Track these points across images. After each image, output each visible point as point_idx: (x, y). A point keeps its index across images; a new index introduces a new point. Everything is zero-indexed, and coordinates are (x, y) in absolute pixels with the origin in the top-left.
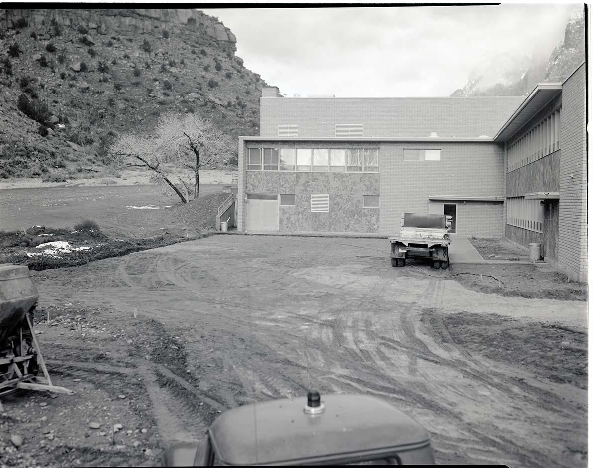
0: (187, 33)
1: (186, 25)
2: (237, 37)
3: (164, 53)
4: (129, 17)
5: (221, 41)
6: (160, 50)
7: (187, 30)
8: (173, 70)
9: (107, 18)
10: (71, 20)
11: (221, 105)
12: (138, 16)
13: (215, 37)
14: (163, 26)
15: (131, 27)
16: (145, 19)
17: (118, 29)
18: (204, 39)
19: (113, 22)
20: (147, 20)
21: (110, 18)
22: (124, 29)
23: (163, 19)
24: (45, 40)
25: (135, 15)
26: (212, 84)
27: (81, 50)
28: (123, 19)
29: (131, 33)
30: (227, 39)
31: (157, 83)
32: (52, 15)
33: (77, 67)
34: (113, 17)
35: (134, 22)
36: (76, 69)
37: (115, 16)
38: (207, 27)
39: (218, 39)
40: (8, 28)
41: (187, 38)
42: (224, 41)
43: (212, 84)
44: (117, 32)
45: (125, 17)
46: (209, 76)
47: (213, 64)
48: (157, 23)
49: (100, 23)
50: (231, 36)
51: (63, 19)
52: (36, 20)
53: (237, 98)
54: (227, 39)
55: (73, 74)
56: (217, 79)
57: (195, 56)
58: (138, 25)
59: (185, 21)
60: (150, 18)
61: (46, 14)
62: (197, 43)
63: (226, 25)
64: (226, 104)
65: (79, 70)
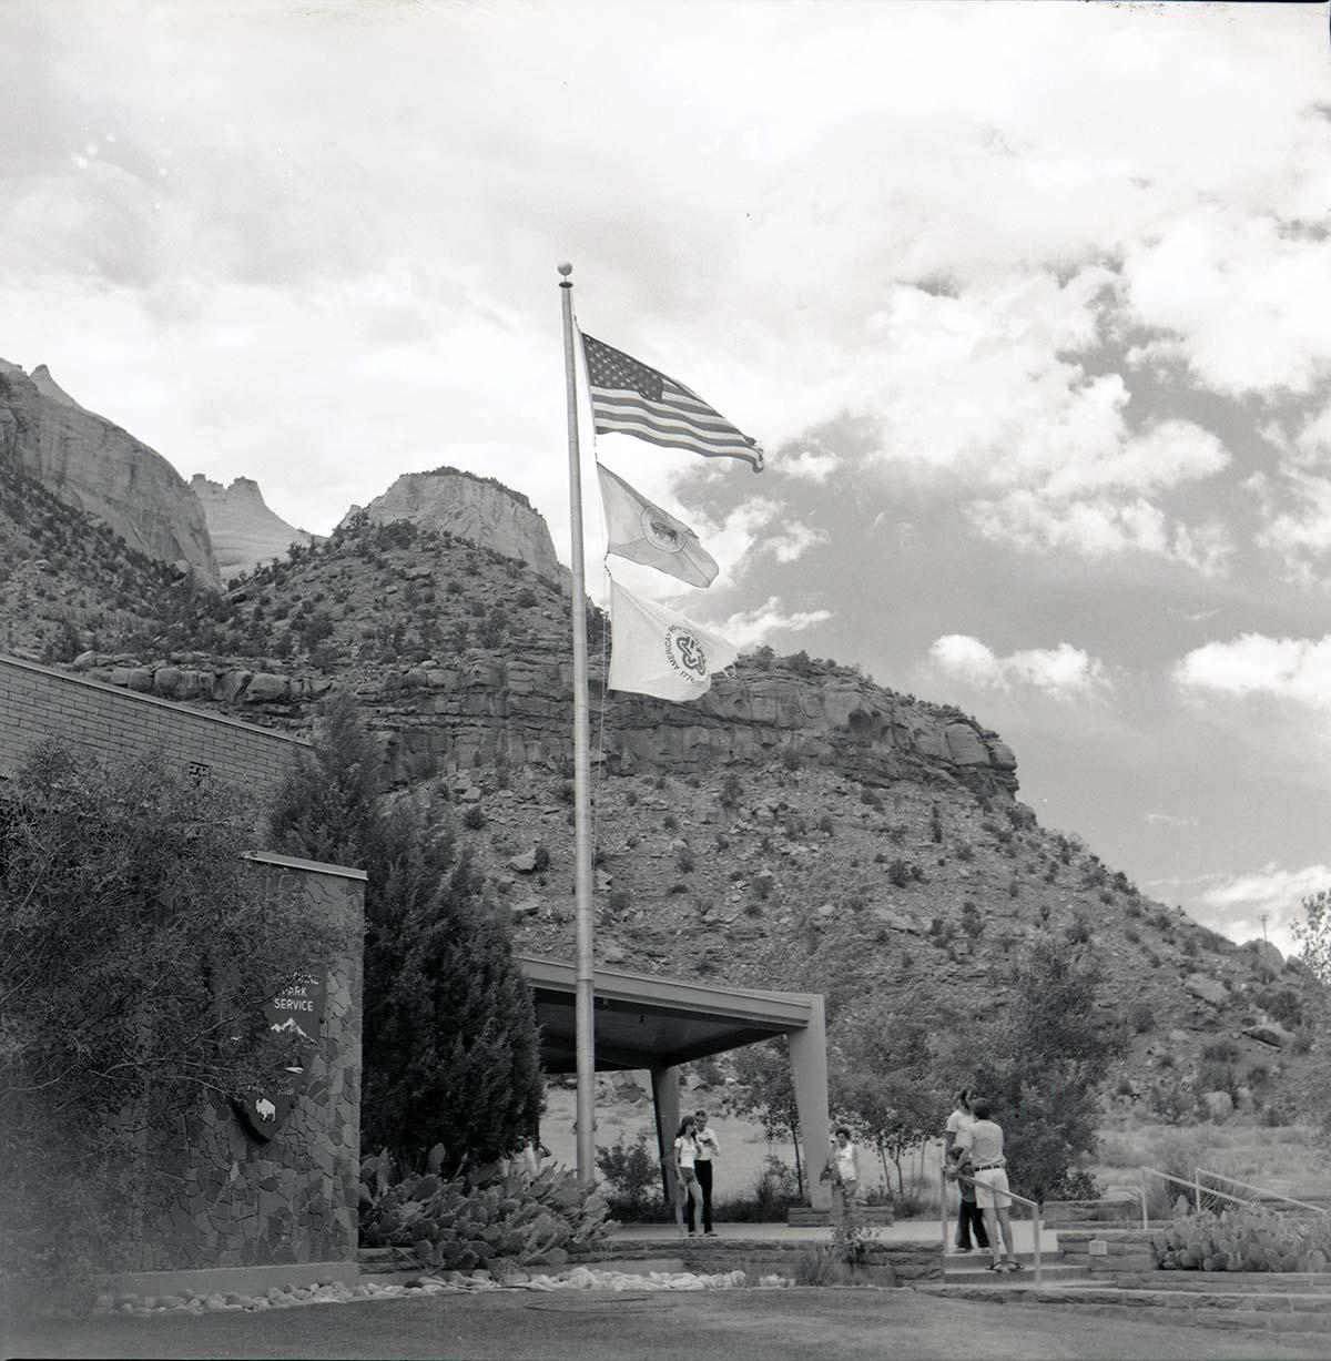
0: (852, 751)
1: (847, 731)
2: (1015, 753)
3: (775, 806)
4: (690, 725)
5: (968, 765)
6: (768, 800)
7: (852, 744)
8: (795, 849)
9: (632, 733)
10: (546, 750)
11: (910, 932)
12: (715, 722)
13: (946, 753)
14: (786, 739)
15: (696, 751)
16: (736, 726)
17: (663, 758)
18: (909, 763)
19: (650, 742)
20: (740, 729)
21: (643, 734)
22: (678, 757)
23: (785, 723)
24: (467, 801)
25: (705, 721)
26: (901, 877)
27: (555, 817)
28: (675, 734)
29: (695, 766)
30: (986, 759)
31: (739, 884)
32: (499, 744)
33: (526, 860)
34: (651, 731)
35: (705, 736)
36: (523, 867)
37: (654, 728)
38: (918, 733)
39: (958, 761)
40: (397, 783)
41: (852, 765)
42: (974, 765)
43: (901, 877)
44: (660, 766)
45: (680, 727)
46: (893, 854)
47: (923, 821)
48: (767, 735)
49: (619, 747)
50: (998, 751)
51: (526, 746)
52: (462, 758)
53: (969, 908)
54: (986, 759)
55: (506, 879)
56: (927, 862)
57: (868, 809)
58: (715, 744)
59: (843, 720)
60: (752, 723)
61: (483, 739)
62: (883, 775)
63: (986, 724)
64: (929, 926)
65: (530, 868)
